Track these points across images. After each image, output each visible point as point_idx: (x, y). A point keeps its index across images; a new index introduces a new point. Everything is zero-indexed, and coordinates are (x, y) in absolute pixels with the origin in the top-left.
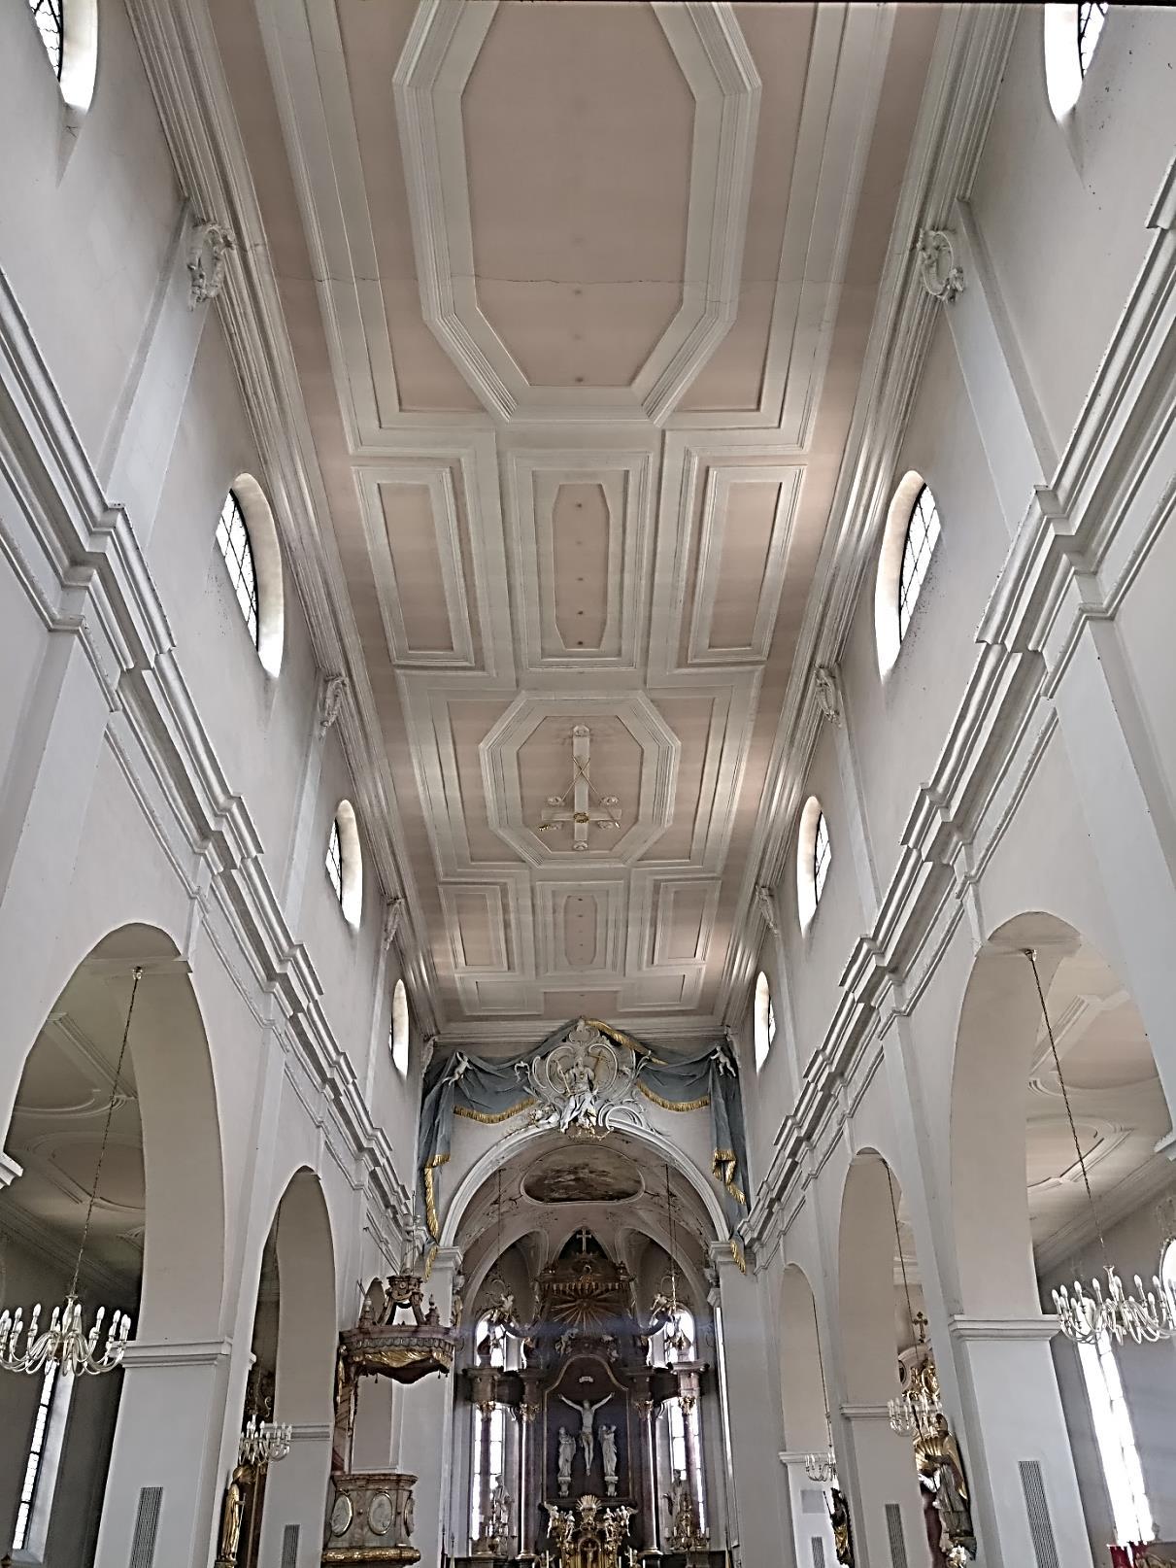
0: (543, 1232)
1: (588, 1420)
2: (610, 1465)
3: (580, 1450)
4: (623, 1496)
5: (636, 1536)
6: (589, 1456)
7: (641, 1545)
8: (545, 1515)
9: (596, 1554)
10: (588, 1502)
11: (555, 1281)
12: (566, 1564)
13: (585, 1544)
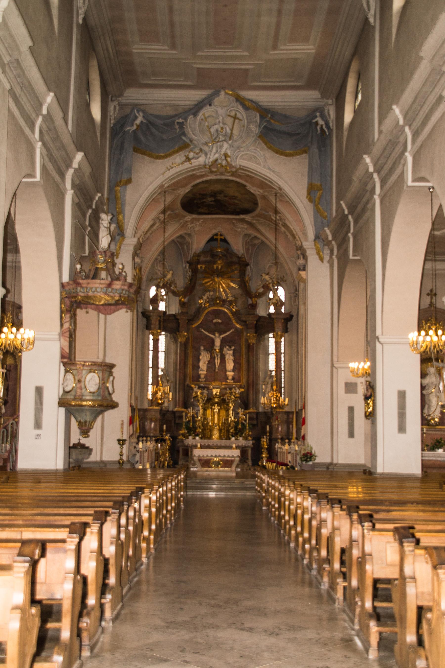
1: (218, 343)
3: (212, 359)
6: (218, 362)
12: (82, 665)
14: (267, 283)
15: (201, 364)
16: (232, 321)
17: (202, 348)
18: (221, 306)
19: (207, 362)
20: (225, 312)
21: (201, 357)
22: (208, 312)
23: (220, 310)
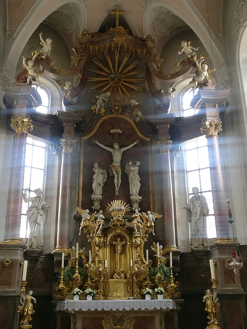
0: (82, 6)
1: (117, 157)
2: (135, 188)
3: (110, 178)
4: (144, 208)
5: (159, 235)
6: (117, 182)
7: (164, 243)
8: (78, 219)
9: (124, 247)
10: (117, 206)
11: (91, 43)
13: (114, 238)
14: (189, 56)
15: (94, 186)
16: (135, 132)
17: (96, 165)
18: (120, 114)
19: (102, 185)
20: (127, 121)
21: (94, 177)
22: (104, 121)
23: (119, 118)
